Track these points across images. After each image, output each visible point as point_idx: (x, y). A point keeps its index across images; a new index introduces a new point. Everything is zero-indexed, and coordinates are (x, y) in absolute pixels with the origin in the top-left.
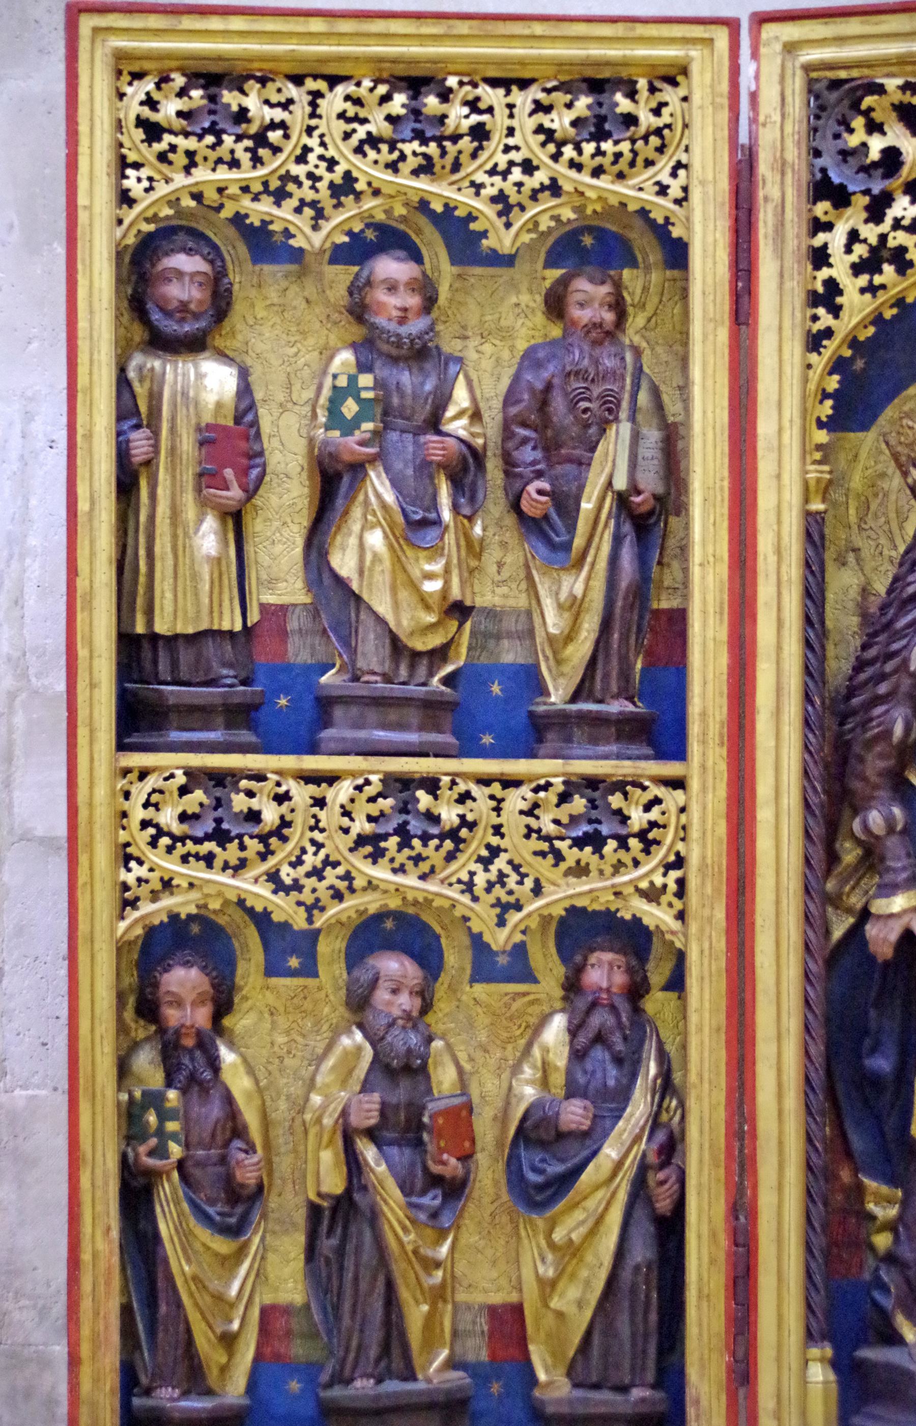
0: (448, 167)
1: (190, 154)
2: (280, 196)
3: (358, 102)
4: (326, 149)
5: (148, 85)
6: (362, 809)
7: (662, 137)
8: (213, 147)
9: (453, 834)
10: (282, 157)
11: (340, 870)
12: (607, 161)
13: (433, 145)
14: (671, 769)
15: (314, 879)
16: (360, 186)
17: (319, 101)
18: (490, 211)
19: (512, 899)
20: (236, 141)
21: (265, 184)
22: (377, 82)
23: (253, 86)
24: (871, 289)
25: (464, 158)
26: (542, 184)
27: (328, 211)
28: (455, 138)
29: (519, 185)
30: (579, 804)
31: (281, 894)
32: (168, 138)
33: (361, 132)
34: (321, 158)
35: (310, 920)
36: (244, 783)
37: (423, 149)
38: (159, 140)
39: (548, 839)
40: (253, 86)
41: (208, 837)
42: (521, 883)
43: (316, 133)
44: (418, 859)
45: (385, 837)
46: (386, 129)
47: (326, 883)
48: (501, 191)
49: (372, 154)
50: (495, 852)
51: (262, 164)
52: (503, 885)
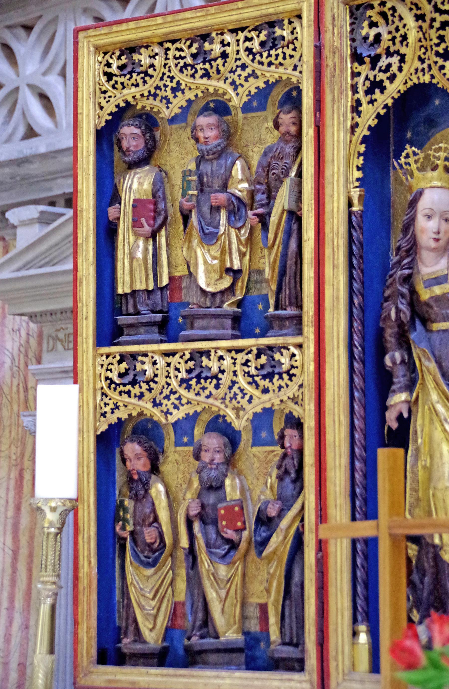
0: (215, 72)
1: (122, 84)
2: (155, 96)
3: (181, 50)
4: (171, 73)
5: (107, 57)
6: (183, 367)
7: (294, 44)
8: (129, 79)
9: (215, 377)
10: (153, 79)
11: (177, 396)
12: (273, 59)
13: (207, 64)
14: (298, 340)
15: (166, 400)
16: (183, 87)
17: (168, 52)
18: (230, 90)
19: (239, 405)
20: (137, 75)
21: (149, 92)
22: (187, 40)
23: (143, 50)
24: (372, 102)
25: (221, 68)
26: (249, 74)
27: (172, 100)
28: (215, 60)
29: (240, 76)
30: (263, 359)
31: (156, 407)
32: (115, 78)
33: (182, 62)
34: (169, 77)
35: (166, 419)
36: (140, 358)
37: (204, 66)
38: (111, 80)
39: (252, 376)
40: (143, 50)
41: (129, 384)
42: (243, 398)
43: (167, 67)
44: (203, 389)
45: (191, 379)
46: (189, 60)
47: (171, 402)
48: (233, 80)
49: (185, 71)
50: (234, 383)
51: (147, 83)
52: (236, 399)
